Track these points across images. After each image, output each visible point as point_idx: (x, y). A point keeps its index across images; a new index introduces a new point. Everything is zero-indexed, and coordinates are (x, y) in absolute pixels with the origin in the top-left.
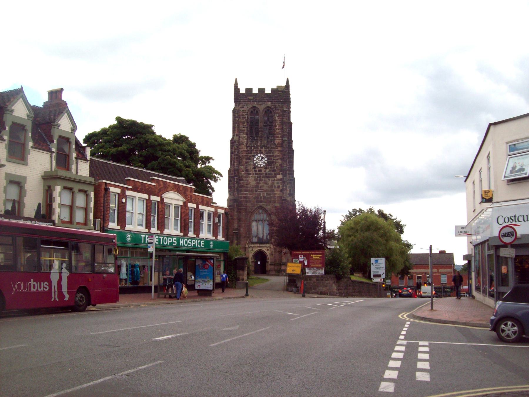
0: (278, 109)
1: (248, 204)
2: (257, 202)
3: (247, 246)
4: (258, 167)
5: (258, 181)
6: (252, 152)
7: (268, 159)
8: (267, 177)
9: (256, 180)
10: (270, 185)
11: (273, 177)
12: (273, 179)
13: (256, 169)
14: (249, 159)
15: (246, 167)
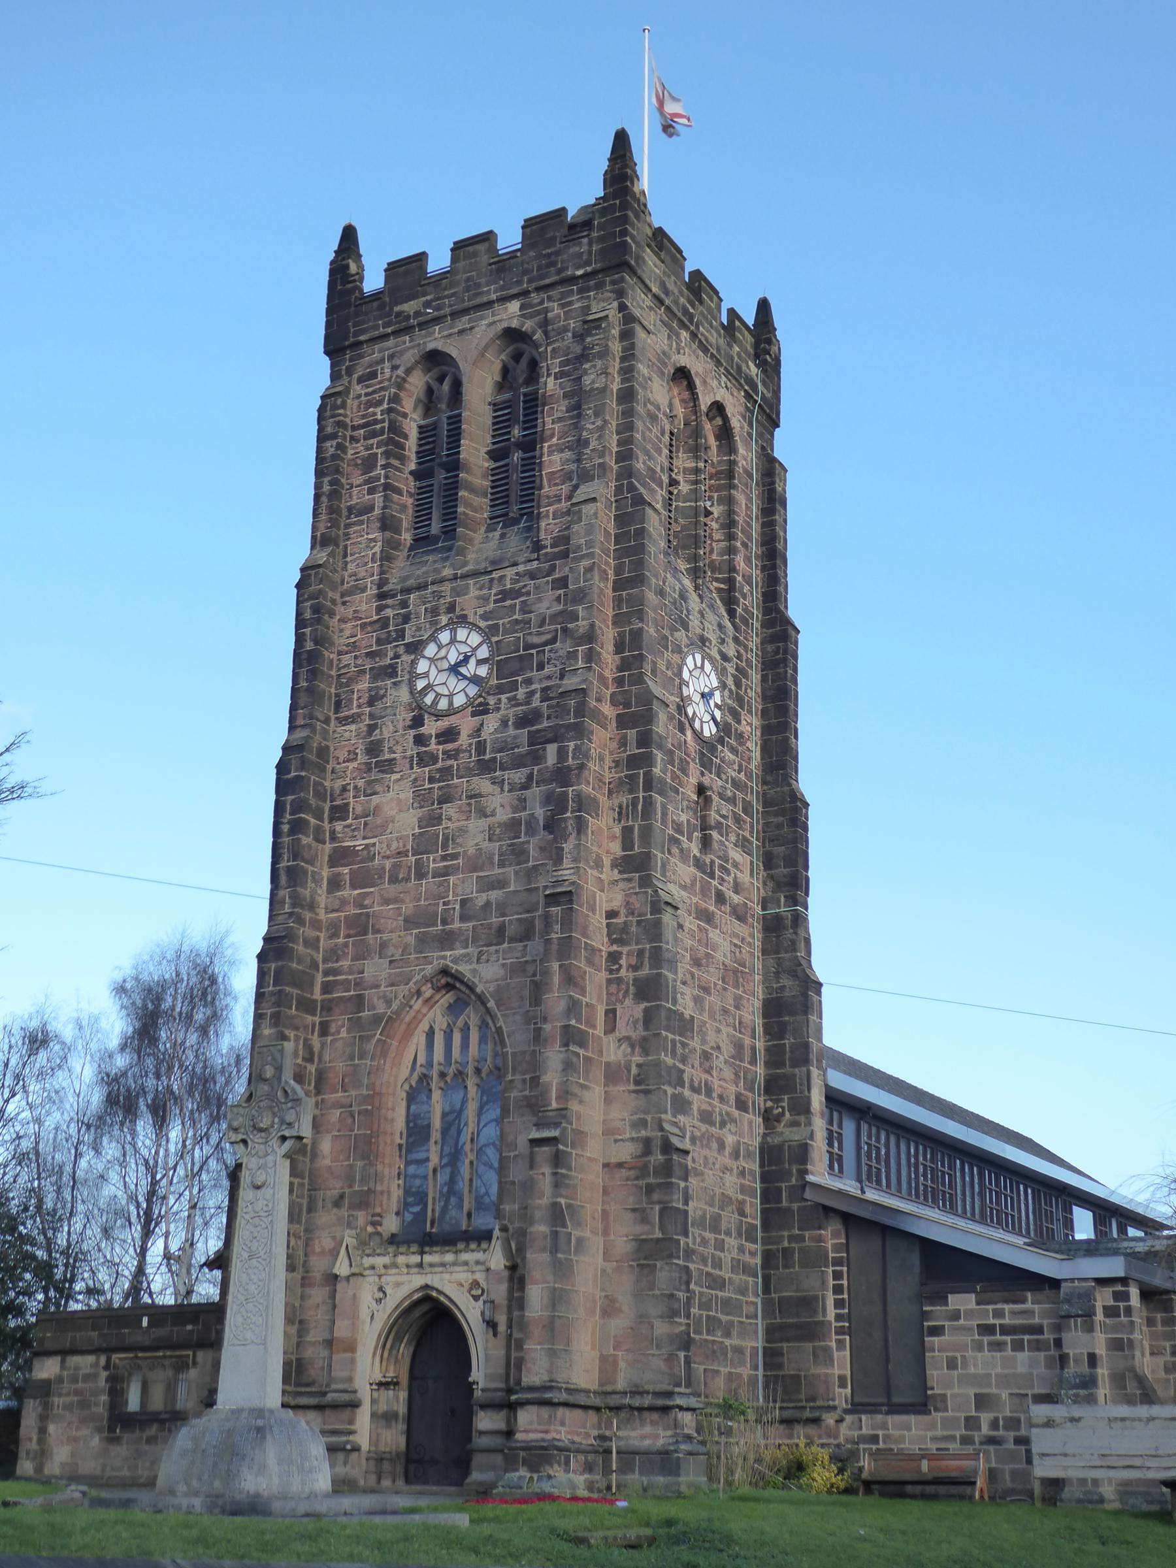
0: (565, 329)
1: (376, 969)
2: (422, 940)
3: (342, 1268)
4: (439, 716)
5: (434, 801)
6: (409, 629)
7: (496, 648)
8: (486, 767)
9: (421, 798)
10: (503, 815)
11: (518, 763)
12: (518, 776)
13: (431, 727)
14: (391, 671)
15: (372, 728)
